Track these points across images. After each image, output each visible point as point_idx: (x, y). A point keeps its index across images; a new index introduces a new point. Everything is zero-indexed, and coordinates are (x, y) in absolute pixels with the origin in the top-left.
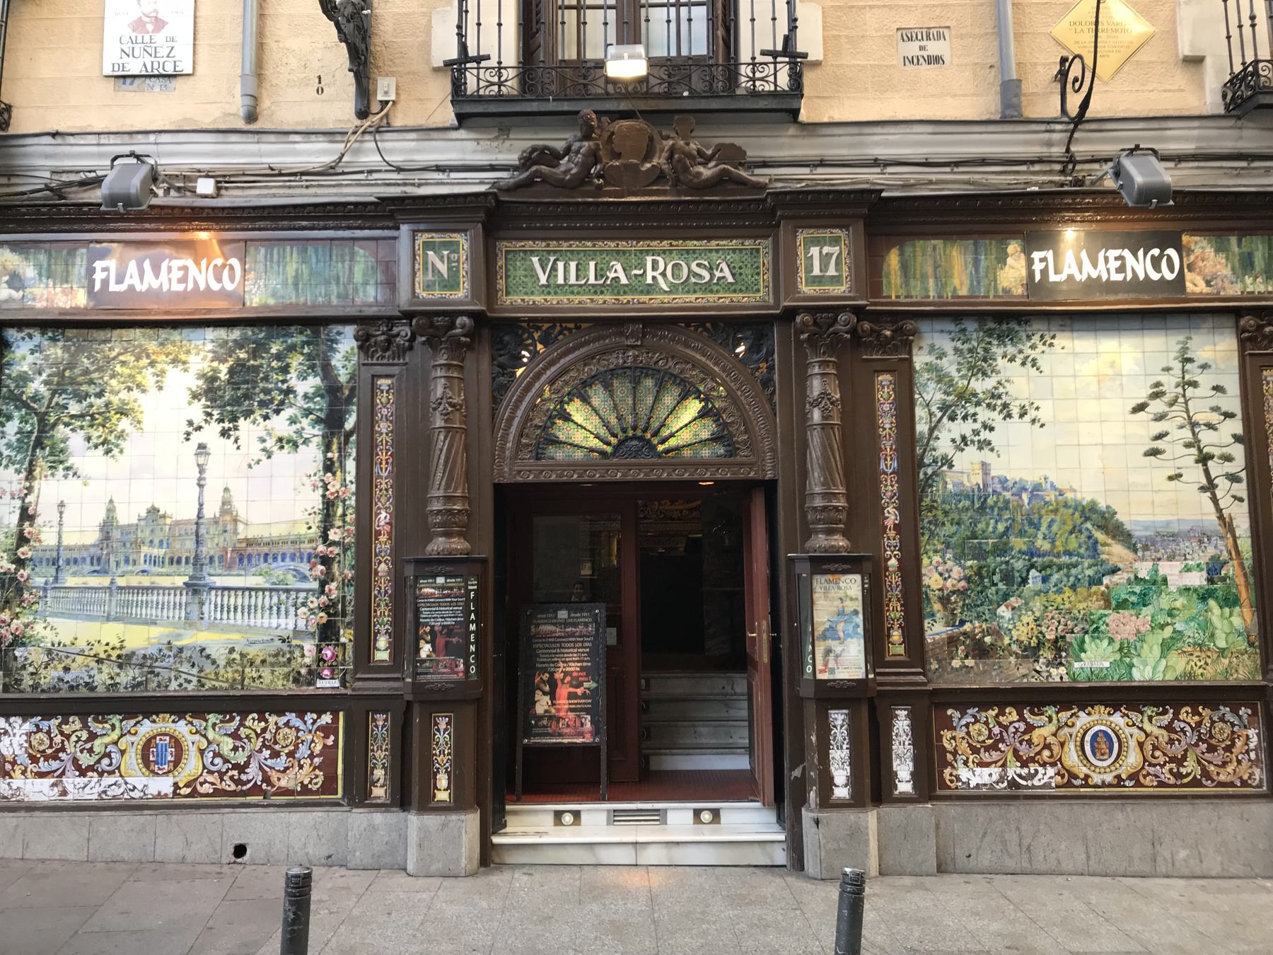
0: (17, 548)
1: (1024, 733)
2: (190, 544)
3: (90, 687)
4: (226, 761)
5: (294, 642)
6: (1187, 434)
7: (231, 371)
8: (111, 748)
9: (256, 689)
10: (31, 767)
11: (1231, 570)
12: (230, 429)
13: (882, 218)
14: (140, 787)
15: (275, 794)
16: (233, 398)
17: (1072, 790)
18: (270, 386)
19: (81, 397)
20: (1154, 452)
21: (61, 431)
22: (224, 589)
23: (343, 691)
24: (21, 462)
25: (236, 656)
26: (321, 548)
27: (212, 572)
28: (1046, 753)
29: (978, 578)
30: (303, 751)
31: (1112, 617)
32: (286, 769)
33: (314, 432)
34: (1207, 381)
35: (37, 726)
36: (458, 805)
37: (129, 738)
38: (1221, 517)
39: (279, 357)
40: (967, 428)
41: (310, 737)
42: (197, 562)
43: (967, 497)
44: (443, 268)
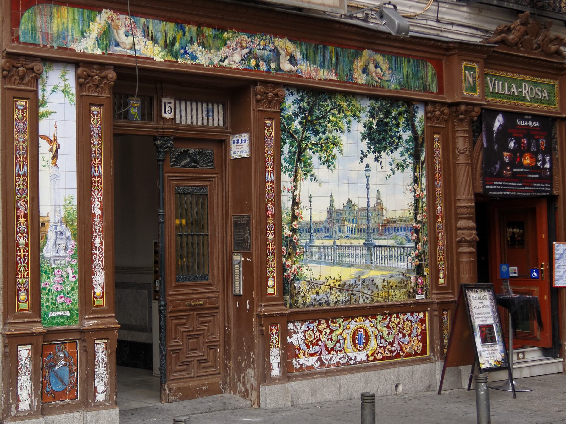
2: (365, 222)
4: (386, 341)
7: (377, 125)
8: (340, 337)
12: (378, 157)
15: (405, 357)
18: (393, 134)
19: (316, 133)
23: (426, 300)
24: (291, 170)
25: (386, 283)
26: (415, 225)
30: (414, 333)
32: (408, 343)
33: (410, 161)
35: (308, 327)
37: (346, 331)
39: (395, 118)
41: (416, 325)
42: (368, 231)
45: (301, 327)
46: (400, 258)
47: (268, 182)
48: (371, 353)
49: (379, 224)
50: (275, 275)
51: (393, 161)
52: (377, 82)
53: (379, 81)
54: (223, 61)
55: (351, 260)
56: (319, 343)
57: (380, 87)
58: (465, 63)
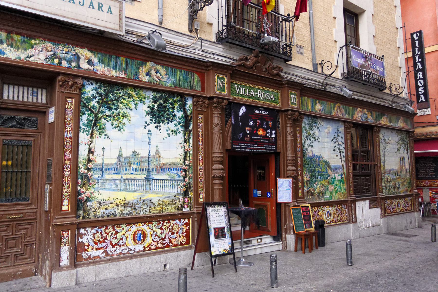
0: (87, 164)
2: (146, 164)
3: (114, 215)
4: (159, 237)
5: (177, 197)
7: (158, 107)
8: (123, 236)
9: (166, 212)
10: (95, 246)
11: (343, 176)
12: (158, 126)
13: (303, 90)
14: (133, 249)
15: (173, 246)
16: (159, 115)
19: (110, 109)
21: (103, 121)
22: (157, 180)
23: (190, 212)
24: (88, 131)
25: (161, 202)
26: (184, 167)
27: (153, 174)
29: (311, 177)
30: (181, 232)
31: (330, 186)
32: (176, 238)
35: (97, 231)
37: (128, 232)
39: (171, 104)
41: (182, 227)
42: (148, 170)
43: (310, 158)
44: (221, 85)
45: (91, 231)
47: (67, 138)
48: (147, 245)
49: (157, 166)
50: (70, 198)
51: (169, 129)
52: (157, 81)
53: (159, 81)
54: (30, 58)
55: (135, 188)
56: (106, 241)
57: (159, 84)
58: (218, 74)
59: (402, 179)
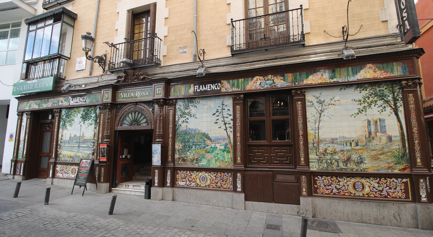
1: (338, 182)
6: (222, 119)
16: (85, 118)
17: (198, 187)
19: (69, 118)
20: (216, 123)
28: (344, 187)
29: (184, 147)
31: (207, 154)
33: (94, 122)
34: (226, 108)
36: (105, 182)
38: (228, 135)
40: (184, 119)
42: (79, 143)
46: (88, 150)
59: (373, 150)
